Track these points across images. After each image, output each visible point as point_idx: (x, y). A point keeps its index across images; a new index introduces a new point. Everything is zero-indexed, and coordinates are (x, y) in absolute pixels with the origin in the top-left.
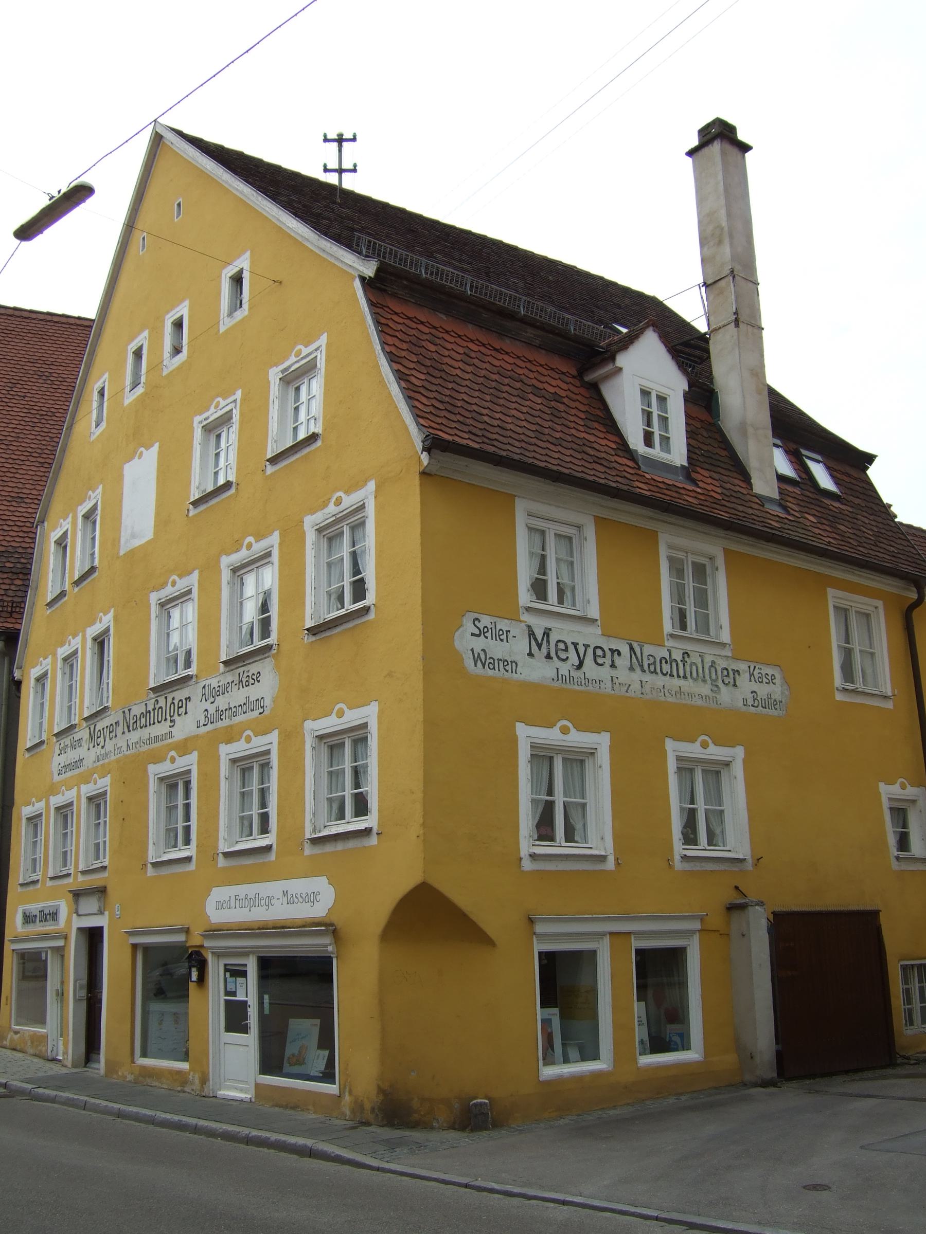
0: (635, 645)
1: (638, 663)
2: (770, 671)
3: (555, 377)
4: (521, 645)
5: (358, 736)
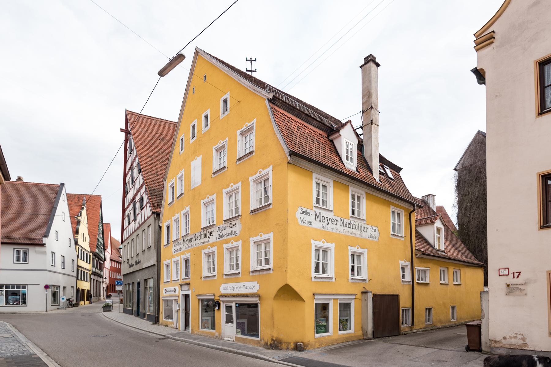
1: (343, 225)
4: (313, 217)
5: (267, 242)
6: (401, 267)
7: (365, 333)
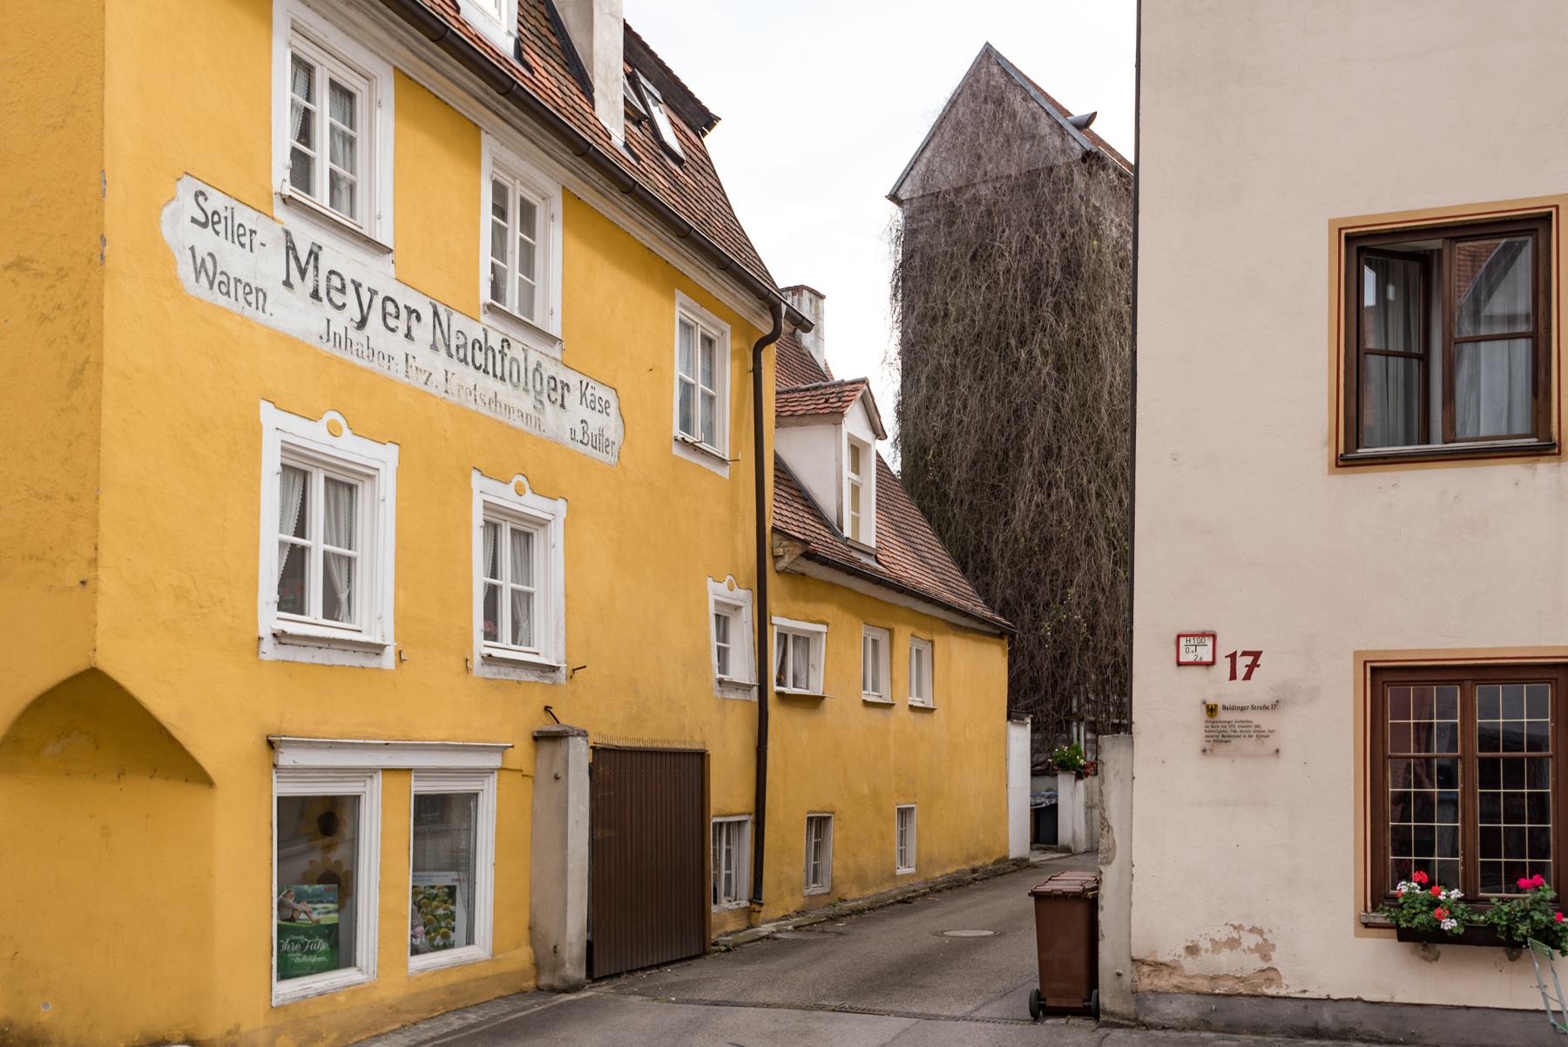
0: (441, 309)
1: (443, 343)
4: (268, 266)
6: (712, 610)
7: (545, 956)
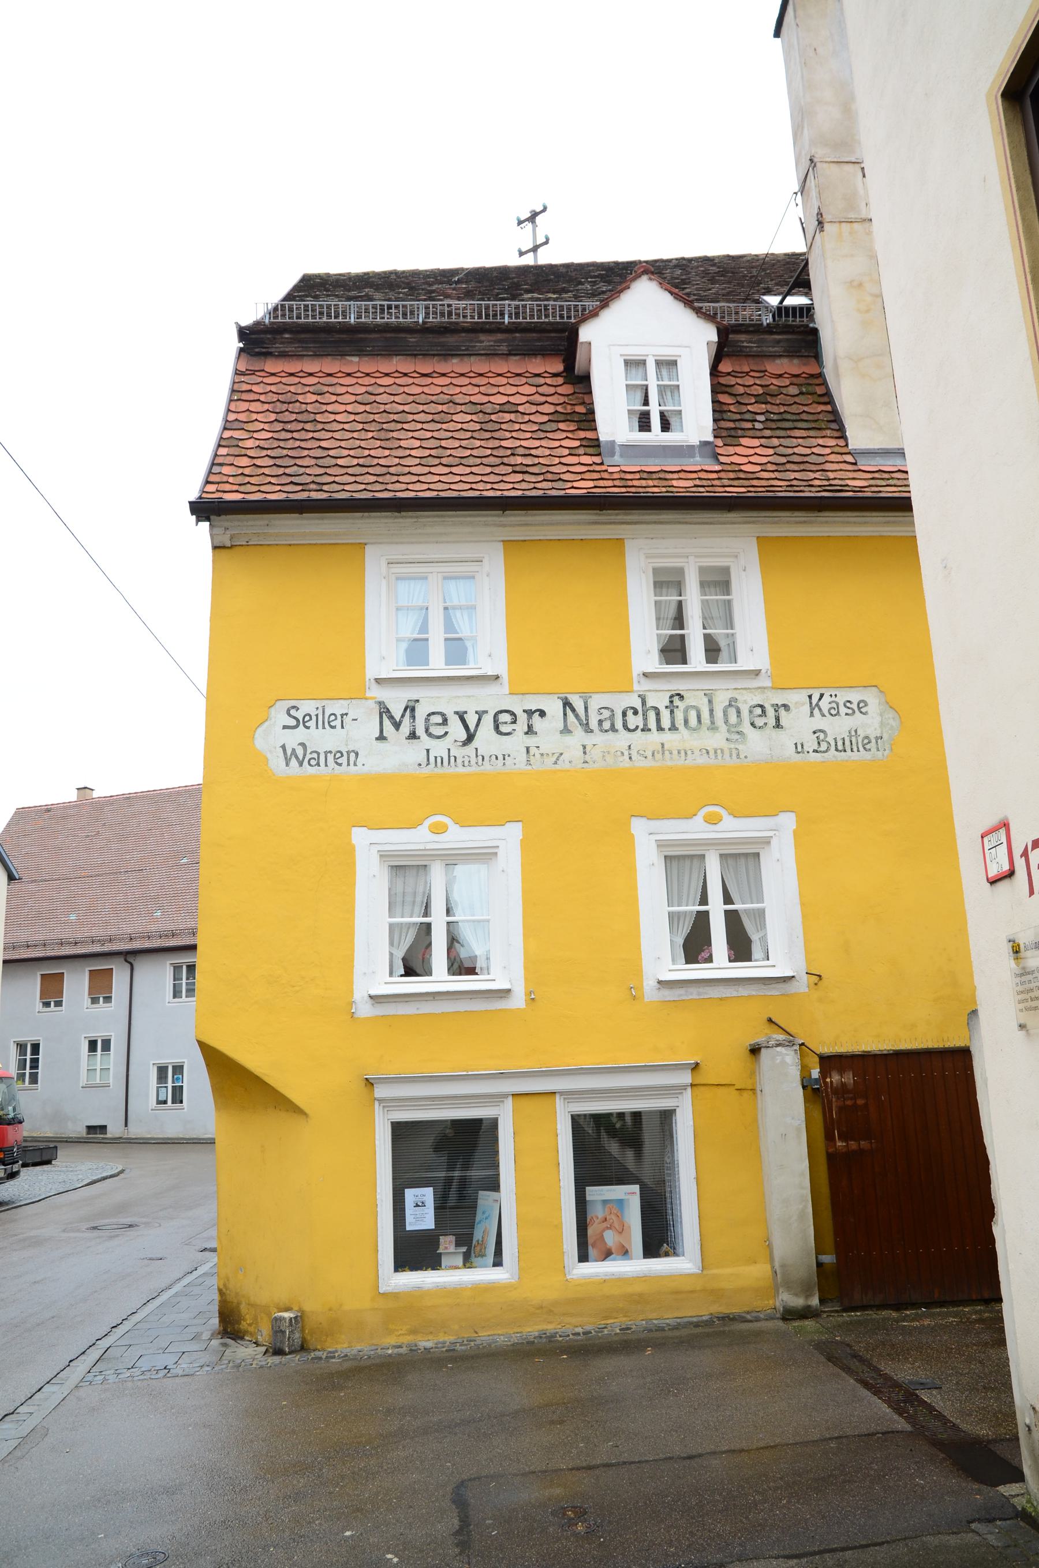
2: (855, 697)
3: (524, 385)
